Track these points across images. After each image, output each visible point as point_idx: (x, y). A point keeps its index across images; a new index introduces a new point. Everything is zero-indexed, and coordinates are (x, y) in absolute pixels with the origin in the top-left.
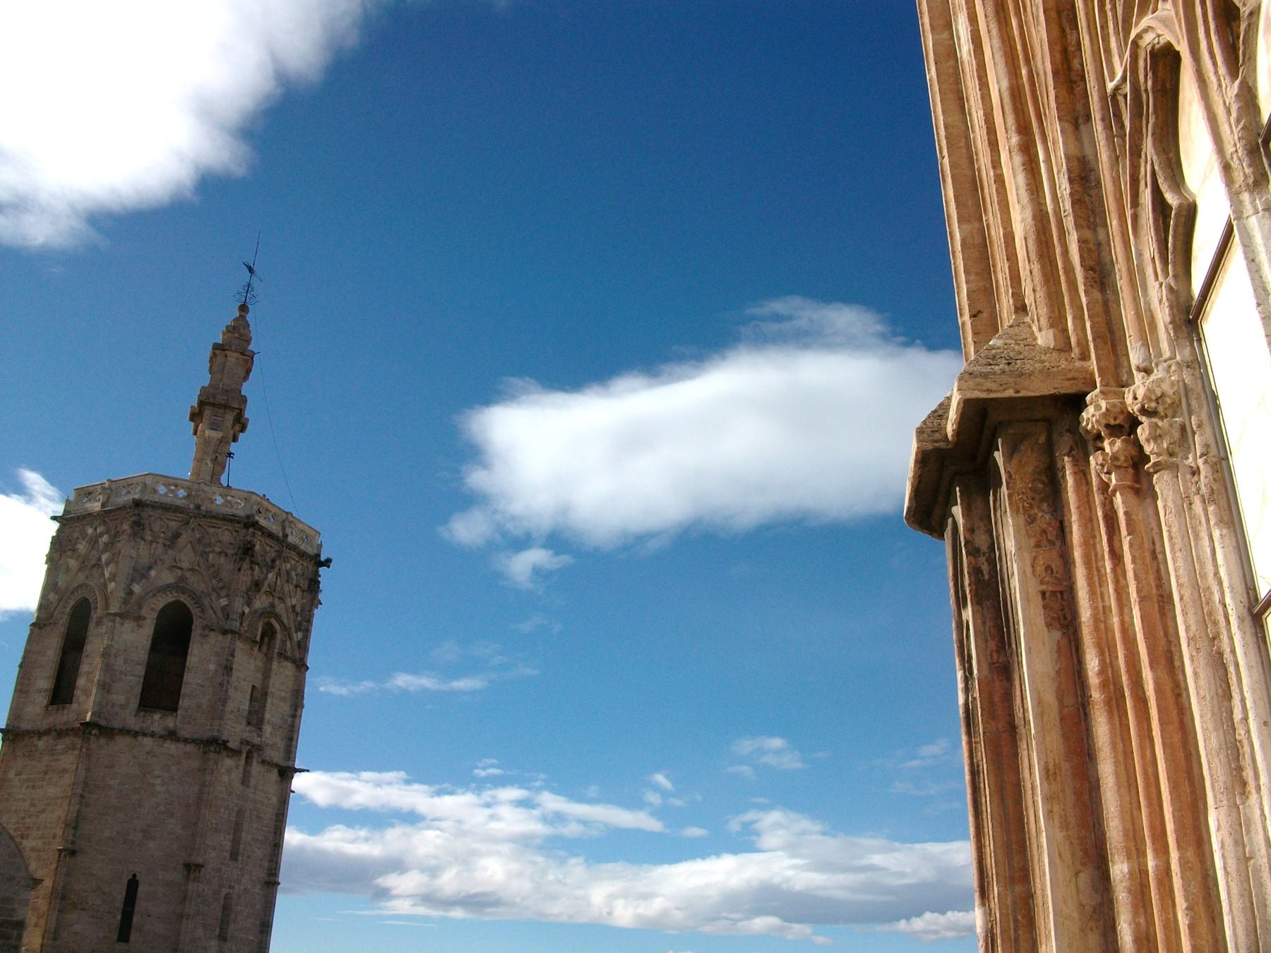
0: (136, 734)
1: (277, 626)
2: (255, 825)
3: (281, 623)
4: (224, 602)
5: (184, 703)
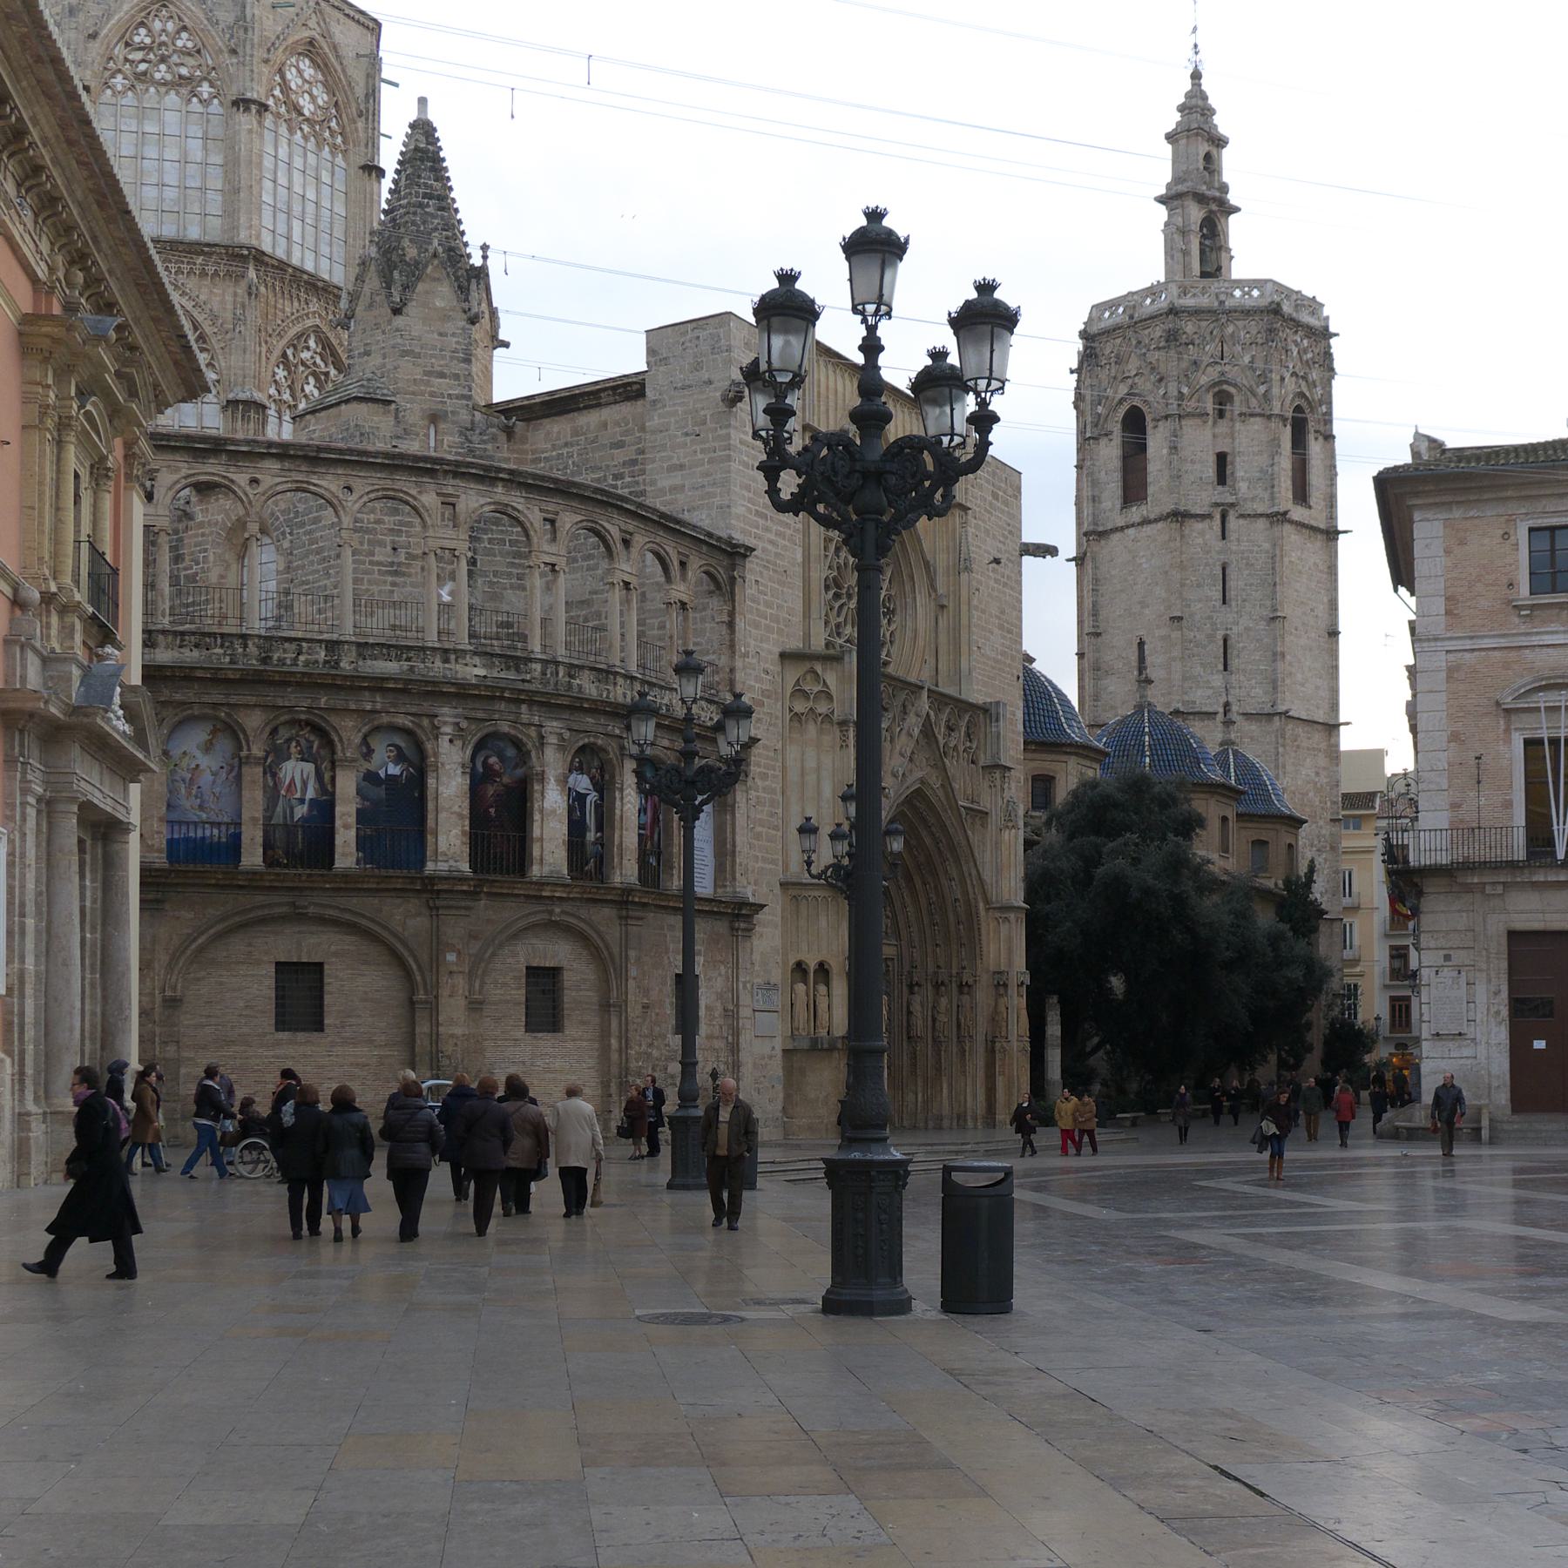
0: (1122, 529)
1: (1232, 390)
3: (1235, 385)
4: (1162, 392)
5: (1150, 490)
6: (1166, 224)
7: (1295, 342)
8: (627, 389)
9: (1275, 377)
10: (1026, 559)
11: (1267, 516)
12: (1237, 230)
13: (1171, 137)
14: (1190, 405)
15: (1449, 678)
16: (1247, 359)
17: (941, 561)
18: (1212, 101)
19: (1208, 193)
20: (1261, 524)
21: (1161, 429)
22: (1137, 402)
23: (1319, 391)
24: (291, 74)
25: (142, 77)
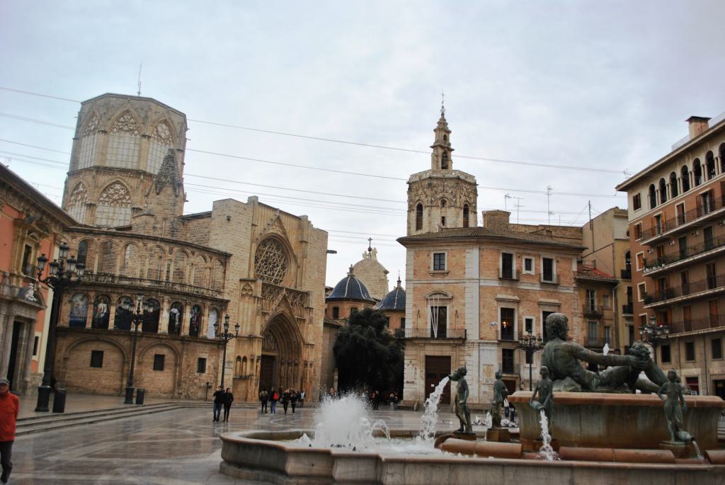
5: (424, 226)
8: (208, 215)
9: (458, 196)
10: (328, 254)
12: (454, 156)
14: (434, 204)
15: (414, 291)
16: (450, 191)
17: (299, 256)
18: (447, 121)
23: (472, 200)
24: (159, 129)
25: (120, 129)
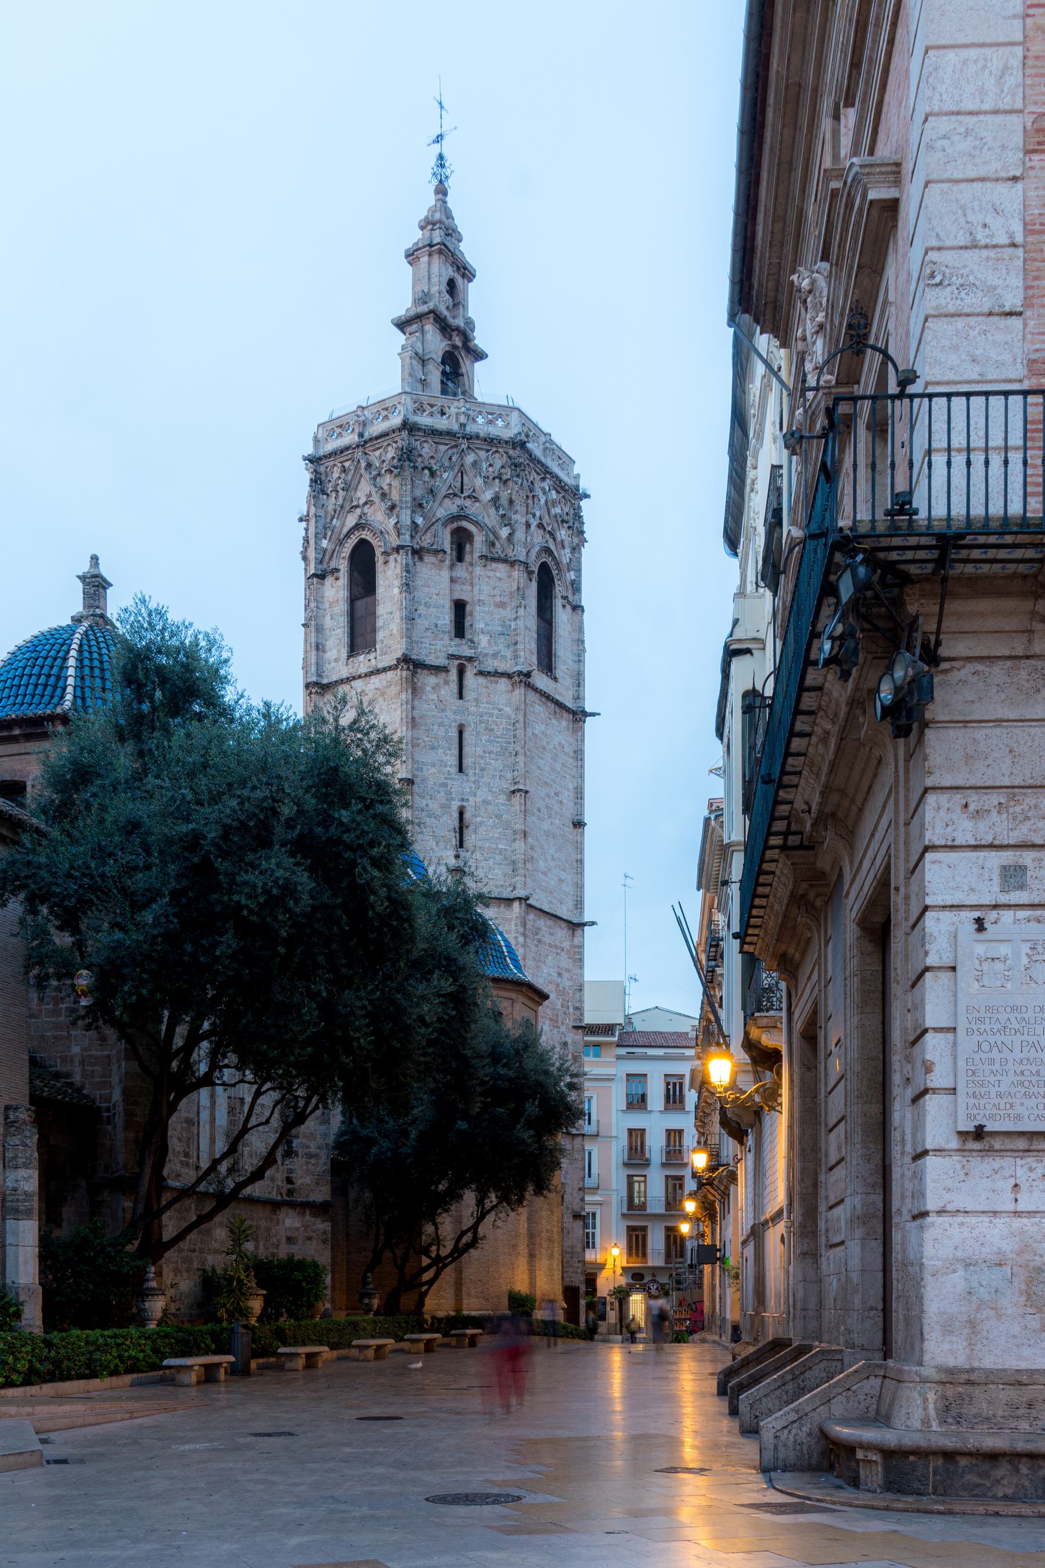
2: (485, 737)
3: (476, 523)
4: (393, 521)
6: (403, 347)
7: (543, 489)
11: (509, 676)
13: (412, 256)
19: (451, 321)
20: (503, 684)
21: (392, 564)
22: (366, 535)
